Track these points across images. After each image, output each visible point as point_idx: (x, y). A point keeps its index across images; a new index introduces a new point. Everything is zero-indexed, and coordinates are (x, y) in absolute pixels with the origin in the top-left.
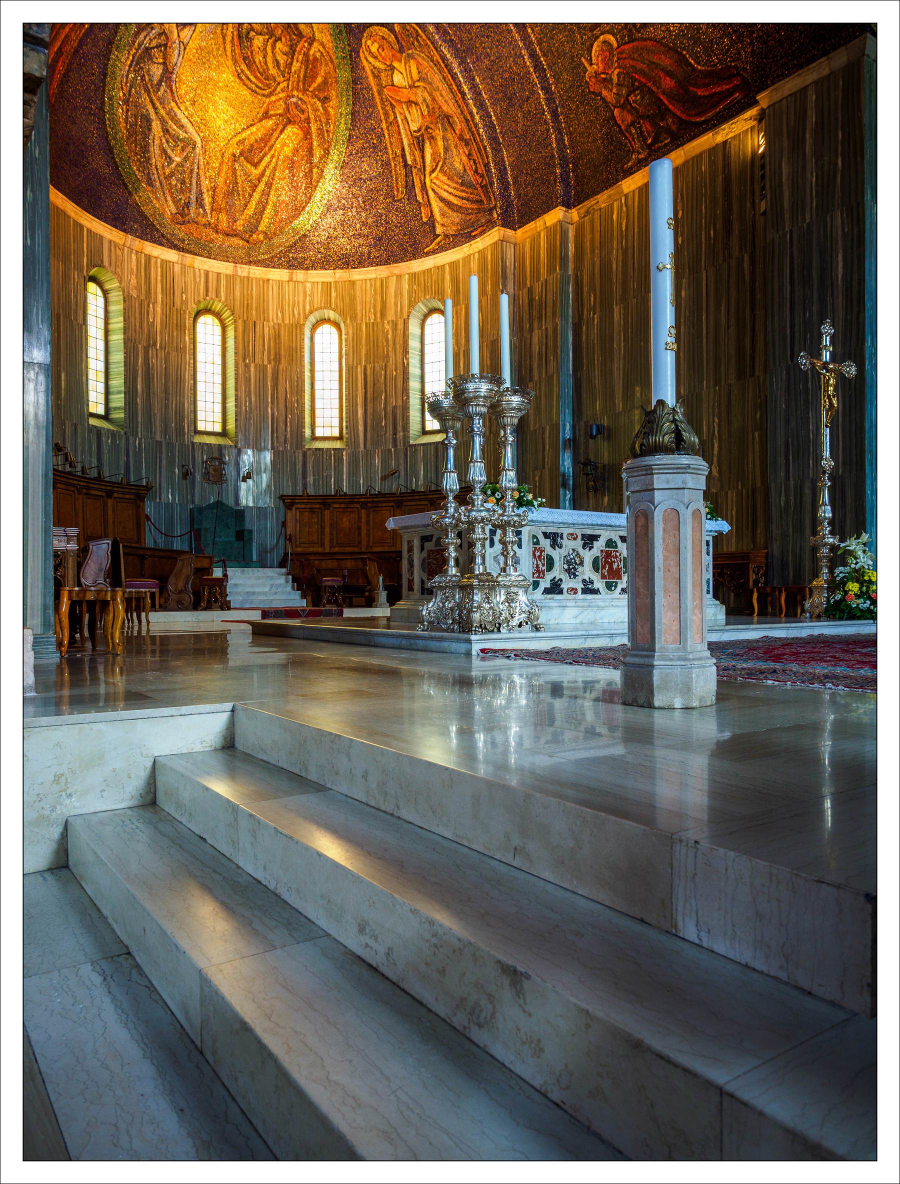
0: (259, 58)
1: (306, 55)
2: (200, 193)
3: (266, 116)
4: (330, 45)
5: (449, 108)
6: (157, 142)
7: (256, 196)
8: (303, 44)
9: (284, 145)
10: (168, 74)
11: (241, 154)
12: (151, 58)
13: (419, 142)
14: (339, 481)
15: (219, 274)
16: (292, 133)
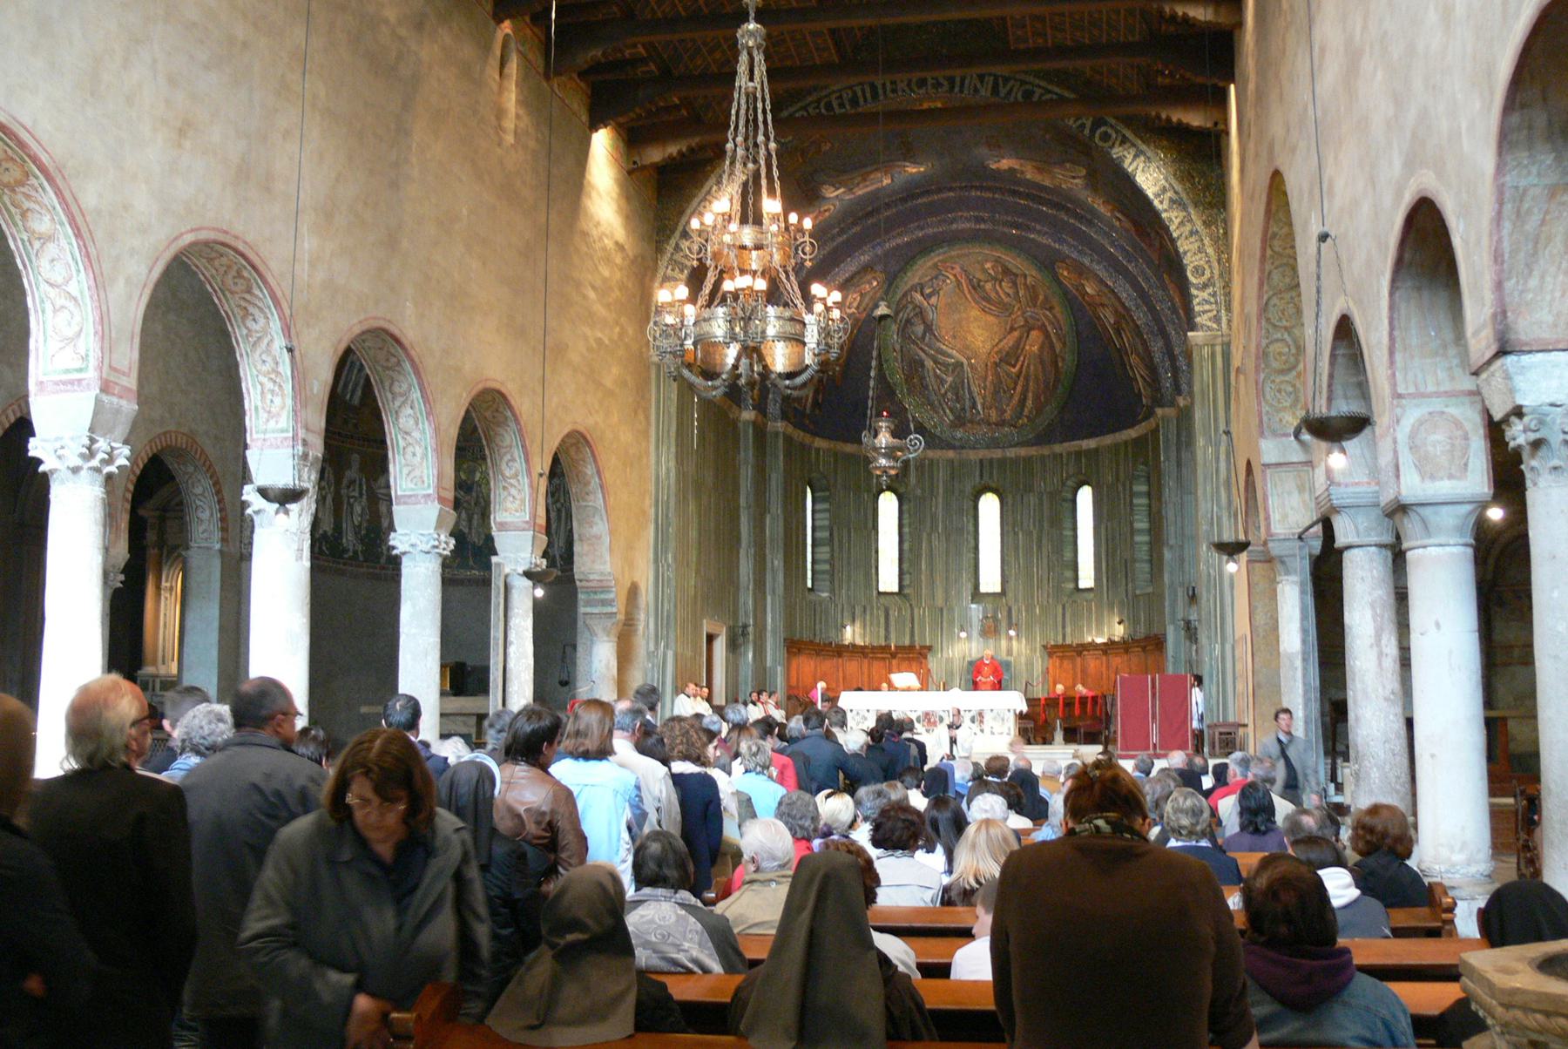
0: (993, 295)
1: (1025, 284)
2: (973, 399)
3: (1012, 329)
4: (1039, 277)
5: (1120, 309)
6: (931, 373)
7: (1019, 388)
8: (1020, 280)
9: (1031, 345)
10: (929, 328)
11: (1001, 360)
12: (912, 324)
13: (1118, 332)
15: (991, 461)
16: (1034, 334)
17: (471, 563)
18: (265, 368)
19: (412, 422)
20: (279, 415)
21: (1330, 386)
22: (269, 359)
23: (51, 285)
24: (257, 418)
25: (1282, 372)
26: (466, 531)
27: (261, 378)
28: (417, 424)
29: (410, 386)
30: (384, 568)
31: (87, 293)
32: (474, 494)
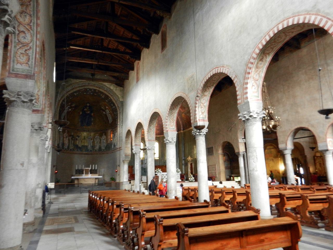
14: (158, 163)
17: (79, 150)
18: (172, 118)
19: (152, 127)
20: (172, 126)
21: (290, 134)
22: (173, 117)
23: (202, 103)
24: (169, 126)
25: (241, 131)
26: (78, 144)
27: (171, 120)
28: (153, 128)
29: (155, 122)
30: (65, 151)
31: (207, 106)
32: (80, 138)
